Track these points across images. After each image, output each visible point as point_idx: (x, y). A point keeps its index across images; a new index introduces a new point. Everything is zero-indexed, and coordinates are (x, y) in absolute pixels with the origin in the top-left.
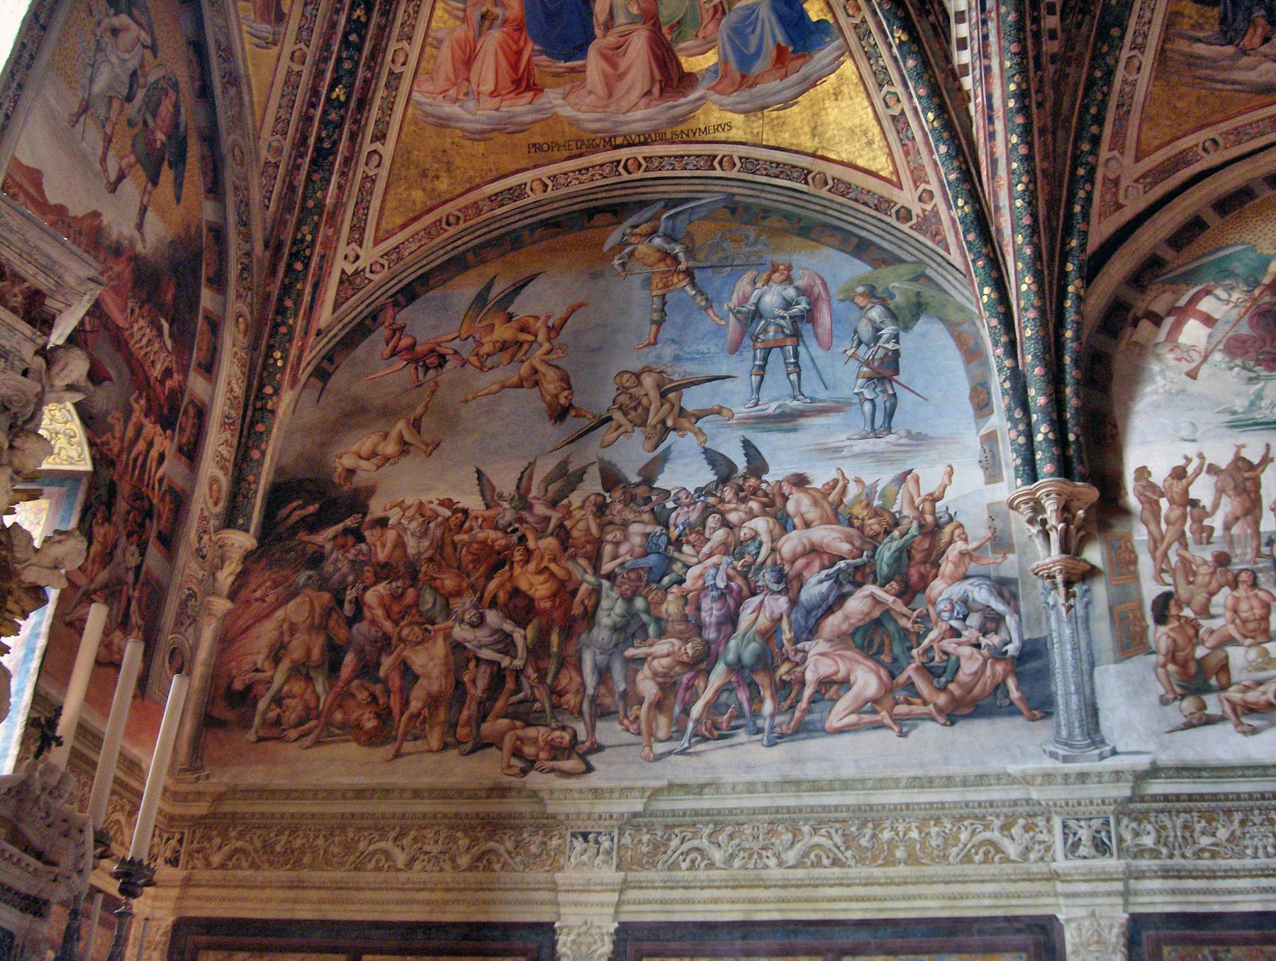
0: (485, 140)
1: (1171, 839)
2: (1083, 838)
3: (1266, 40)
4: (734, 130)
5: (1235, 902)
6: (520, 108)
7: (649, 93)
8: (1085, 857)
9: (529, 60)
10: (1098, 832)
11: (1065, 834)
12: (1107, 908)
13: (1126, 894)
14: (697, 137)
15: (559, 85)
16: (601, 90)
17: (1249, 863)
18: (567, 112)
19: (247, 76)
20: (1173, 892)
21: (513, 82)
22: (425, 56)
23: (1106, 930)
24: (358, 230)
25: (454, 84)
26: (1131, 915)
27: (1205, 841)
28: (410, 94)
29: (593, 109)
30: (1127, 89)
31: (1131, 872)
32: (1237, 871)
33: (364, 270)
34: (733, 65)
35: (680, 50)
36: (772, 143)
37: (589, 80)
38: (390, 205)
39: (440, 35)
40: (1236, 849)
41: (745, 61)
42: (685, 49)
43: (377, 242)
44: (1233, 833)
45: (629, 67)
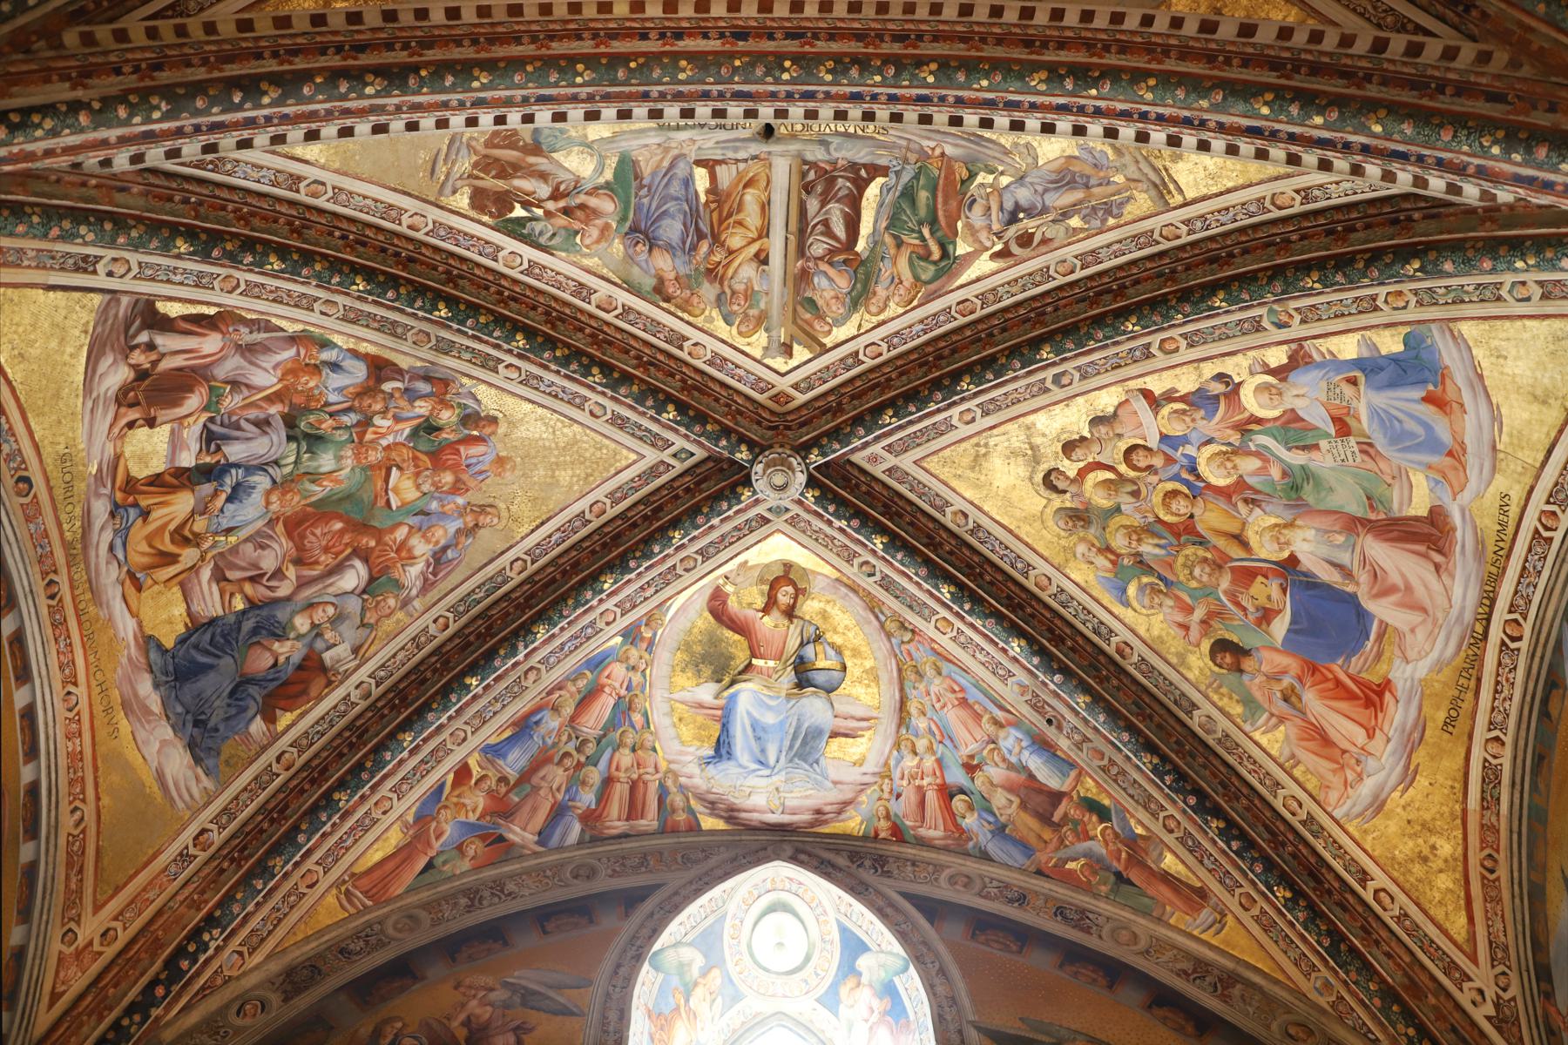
0: (1416, 771)
4: (1511, 493)
6: (1398, 715)
7: (1437, 567)
9: (1349, 676)
14: (1508, 538)
15: (1390, 660)
16: (1415, 617)
18: (1422, 669)
19: (1238, 961)
21: (1367, 707)
22: (1301, 779)
24: (1451, 967)
25: (1342, 767)
28: (1332, 817)
29: (1433, 638)
33: (1498, 996)
34: (1435, 459)
35: (1400, 510)
36: (1541, 457)
37: (1397, 625)
38: (1438, 914)
39: (1287, 753)
41: (1431, 443)
42: (1401, 504)
43: (1474, 960)
45: (1403, 575)
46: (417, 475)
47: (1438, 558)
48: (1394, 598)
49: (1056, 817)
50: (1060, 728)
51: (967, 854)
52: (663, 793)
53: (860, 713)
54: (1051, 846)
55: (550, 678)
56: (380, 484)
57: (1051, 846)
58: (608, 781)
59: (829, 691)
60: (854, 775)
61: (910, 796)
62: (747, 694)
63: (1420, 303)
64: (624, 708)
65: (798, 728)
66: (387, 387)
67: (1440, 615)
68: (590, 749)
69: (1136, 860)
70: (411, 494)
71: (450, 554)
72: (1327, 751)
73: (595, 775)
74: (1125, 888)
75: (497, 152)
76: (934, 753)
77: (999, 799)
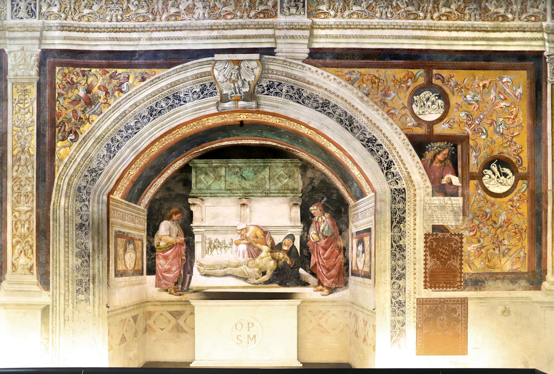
1: (67, 9)
2: (22, 7)
5: (97, 45)
8: (22, 18)
10: (30, 4)
11: (12, 4)
12: (30, 46)
13: (41, 39)
17: (107, 24)
20: (65, 38)
23: (29, 58)
26: (42, 50)
27: (86, 11)
31: (44, 27)
32: (101, 28)
40: (101, 17)
44: (101, 8)
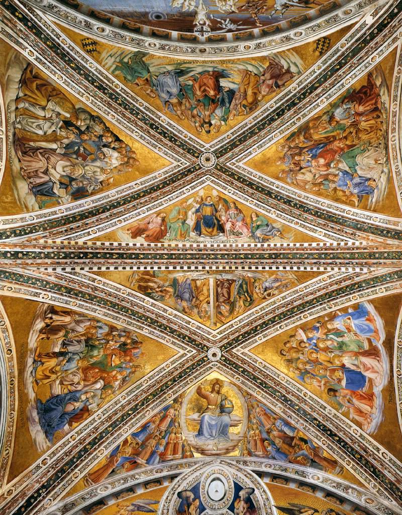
3: (374, 180)
7: (378, 361)
16: (376, 375)
30: (382, 221)
46: (120, 357)
47: (378, 358)
48: (370, 370)
49: (293, 444)
50: (291, 418)
51: (269, 458)
52: (183, 446)
53: (237, 419)
54: (292, 454)
55: (152, 414)
56: (109, 360)
57: (292, 454)
58: (168, 444)
59: (229, 413)
60: (236, 438)
61: (252, 443)
62: (207, 416)
63: (360, 298)
64: (173, 421)
65: (221, 424)
66: (114, 333)
67: (381, 373)
68: (163, 434)
69: (316, 455)
70: (118, 362)
71: (127, 379)
72: (361, 415)
73: (164, 442)
74: (314, 464)
75: (144, 276)
76: (258, 429)
77: (277, 441)
